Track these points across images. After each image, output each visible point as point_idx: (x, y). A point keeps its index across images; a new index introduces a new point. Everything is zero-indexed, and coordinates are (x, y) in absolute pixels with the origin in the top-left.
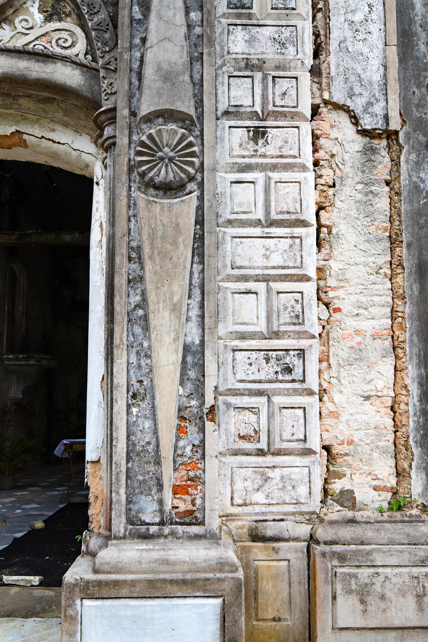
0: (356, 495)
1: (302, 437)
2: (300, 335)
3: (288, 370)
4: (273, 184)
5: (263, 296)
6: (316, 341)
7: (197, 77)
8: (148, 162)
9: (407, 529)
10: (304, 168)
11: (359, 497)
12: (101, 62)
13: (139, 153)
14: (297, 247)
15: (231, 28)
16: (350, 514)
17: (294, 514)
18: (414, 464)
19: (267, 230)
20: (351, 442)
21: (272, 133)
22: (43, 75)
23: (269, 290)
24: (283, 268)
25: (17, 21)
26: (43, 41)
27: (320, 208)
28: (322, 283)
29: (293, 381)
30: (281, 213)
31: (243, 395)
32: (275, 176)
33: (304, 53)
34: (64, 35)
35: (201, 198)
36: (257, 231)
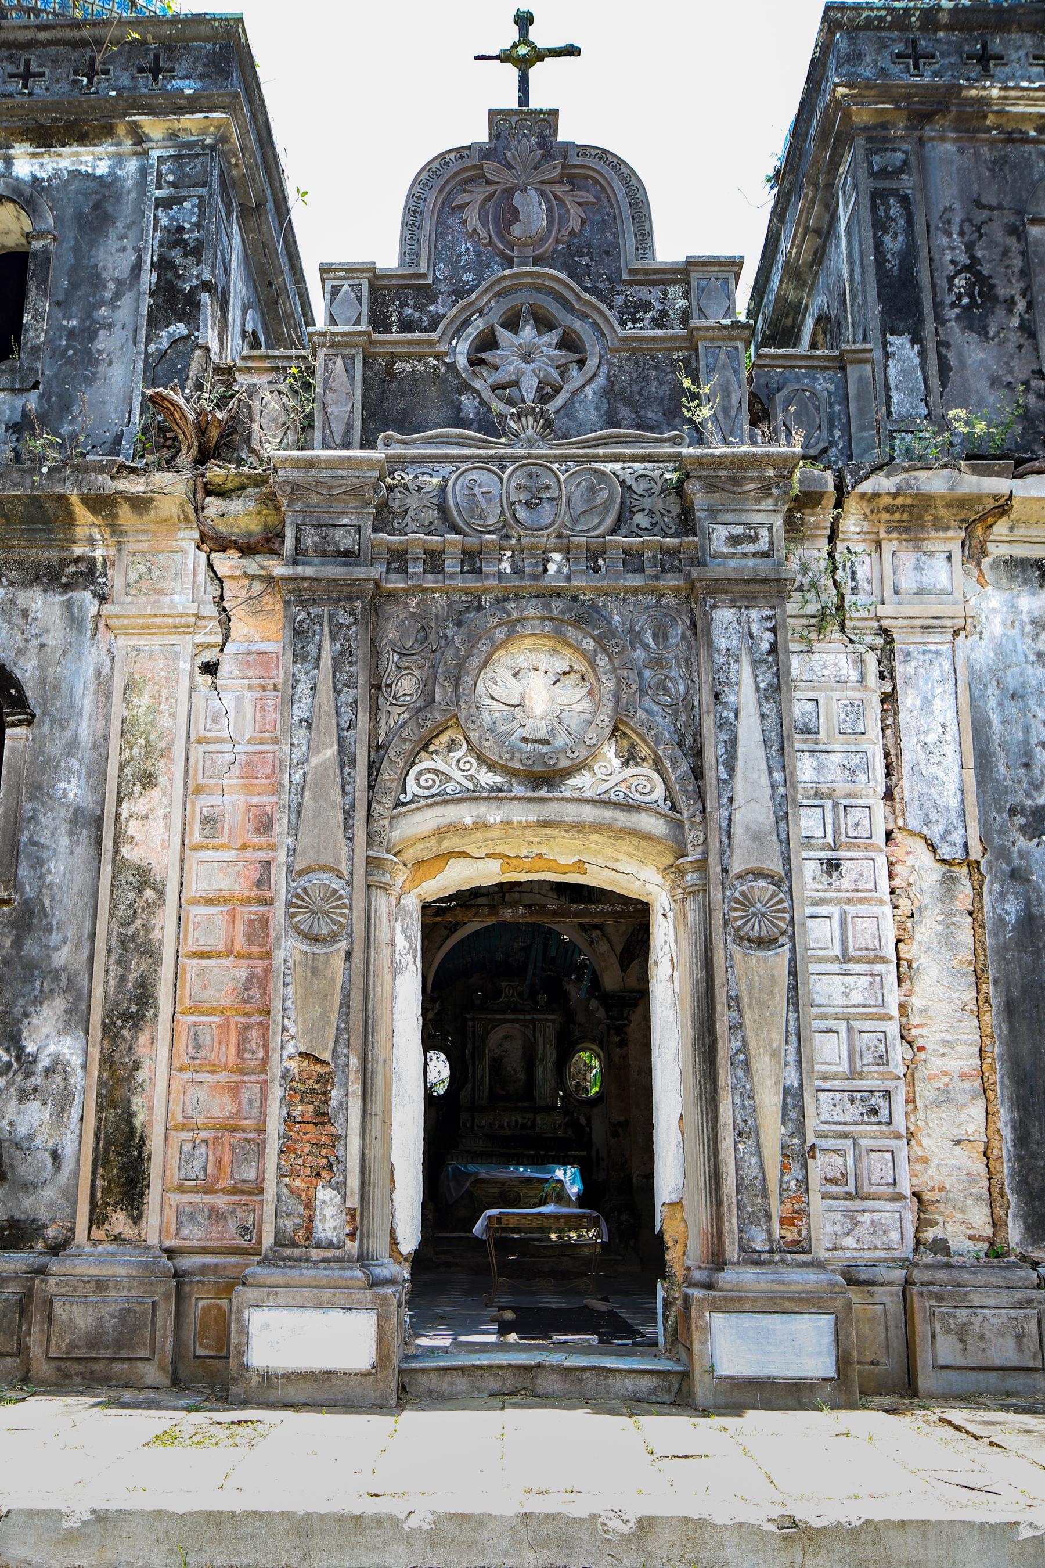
0: (950, 1244)
1: (891, 1180)
2: (883, 1077)
3: (874, 1112)
4: (849, 919)
5: (844, 1035)
6: (902, 1081)
7: (783, 835)
8: (742, 917)
13: (735, 910)
14: (877, 985)
16: (945, 1259)
17: (885, 1260)
19: (845, 966)
21: (846, 865)
22: (629, 824)
23: (849, 1029)
25: (596, 767)
26: (623, 787)
27: (899, 941)
28: (904, 1020)
29: (880, 1123)
30: (859, 949)
31: (827, 1136)
32: (851, 910)
33: (876, 781)
34: (643, 781)
35: (793, 950)
36: (835, 967)
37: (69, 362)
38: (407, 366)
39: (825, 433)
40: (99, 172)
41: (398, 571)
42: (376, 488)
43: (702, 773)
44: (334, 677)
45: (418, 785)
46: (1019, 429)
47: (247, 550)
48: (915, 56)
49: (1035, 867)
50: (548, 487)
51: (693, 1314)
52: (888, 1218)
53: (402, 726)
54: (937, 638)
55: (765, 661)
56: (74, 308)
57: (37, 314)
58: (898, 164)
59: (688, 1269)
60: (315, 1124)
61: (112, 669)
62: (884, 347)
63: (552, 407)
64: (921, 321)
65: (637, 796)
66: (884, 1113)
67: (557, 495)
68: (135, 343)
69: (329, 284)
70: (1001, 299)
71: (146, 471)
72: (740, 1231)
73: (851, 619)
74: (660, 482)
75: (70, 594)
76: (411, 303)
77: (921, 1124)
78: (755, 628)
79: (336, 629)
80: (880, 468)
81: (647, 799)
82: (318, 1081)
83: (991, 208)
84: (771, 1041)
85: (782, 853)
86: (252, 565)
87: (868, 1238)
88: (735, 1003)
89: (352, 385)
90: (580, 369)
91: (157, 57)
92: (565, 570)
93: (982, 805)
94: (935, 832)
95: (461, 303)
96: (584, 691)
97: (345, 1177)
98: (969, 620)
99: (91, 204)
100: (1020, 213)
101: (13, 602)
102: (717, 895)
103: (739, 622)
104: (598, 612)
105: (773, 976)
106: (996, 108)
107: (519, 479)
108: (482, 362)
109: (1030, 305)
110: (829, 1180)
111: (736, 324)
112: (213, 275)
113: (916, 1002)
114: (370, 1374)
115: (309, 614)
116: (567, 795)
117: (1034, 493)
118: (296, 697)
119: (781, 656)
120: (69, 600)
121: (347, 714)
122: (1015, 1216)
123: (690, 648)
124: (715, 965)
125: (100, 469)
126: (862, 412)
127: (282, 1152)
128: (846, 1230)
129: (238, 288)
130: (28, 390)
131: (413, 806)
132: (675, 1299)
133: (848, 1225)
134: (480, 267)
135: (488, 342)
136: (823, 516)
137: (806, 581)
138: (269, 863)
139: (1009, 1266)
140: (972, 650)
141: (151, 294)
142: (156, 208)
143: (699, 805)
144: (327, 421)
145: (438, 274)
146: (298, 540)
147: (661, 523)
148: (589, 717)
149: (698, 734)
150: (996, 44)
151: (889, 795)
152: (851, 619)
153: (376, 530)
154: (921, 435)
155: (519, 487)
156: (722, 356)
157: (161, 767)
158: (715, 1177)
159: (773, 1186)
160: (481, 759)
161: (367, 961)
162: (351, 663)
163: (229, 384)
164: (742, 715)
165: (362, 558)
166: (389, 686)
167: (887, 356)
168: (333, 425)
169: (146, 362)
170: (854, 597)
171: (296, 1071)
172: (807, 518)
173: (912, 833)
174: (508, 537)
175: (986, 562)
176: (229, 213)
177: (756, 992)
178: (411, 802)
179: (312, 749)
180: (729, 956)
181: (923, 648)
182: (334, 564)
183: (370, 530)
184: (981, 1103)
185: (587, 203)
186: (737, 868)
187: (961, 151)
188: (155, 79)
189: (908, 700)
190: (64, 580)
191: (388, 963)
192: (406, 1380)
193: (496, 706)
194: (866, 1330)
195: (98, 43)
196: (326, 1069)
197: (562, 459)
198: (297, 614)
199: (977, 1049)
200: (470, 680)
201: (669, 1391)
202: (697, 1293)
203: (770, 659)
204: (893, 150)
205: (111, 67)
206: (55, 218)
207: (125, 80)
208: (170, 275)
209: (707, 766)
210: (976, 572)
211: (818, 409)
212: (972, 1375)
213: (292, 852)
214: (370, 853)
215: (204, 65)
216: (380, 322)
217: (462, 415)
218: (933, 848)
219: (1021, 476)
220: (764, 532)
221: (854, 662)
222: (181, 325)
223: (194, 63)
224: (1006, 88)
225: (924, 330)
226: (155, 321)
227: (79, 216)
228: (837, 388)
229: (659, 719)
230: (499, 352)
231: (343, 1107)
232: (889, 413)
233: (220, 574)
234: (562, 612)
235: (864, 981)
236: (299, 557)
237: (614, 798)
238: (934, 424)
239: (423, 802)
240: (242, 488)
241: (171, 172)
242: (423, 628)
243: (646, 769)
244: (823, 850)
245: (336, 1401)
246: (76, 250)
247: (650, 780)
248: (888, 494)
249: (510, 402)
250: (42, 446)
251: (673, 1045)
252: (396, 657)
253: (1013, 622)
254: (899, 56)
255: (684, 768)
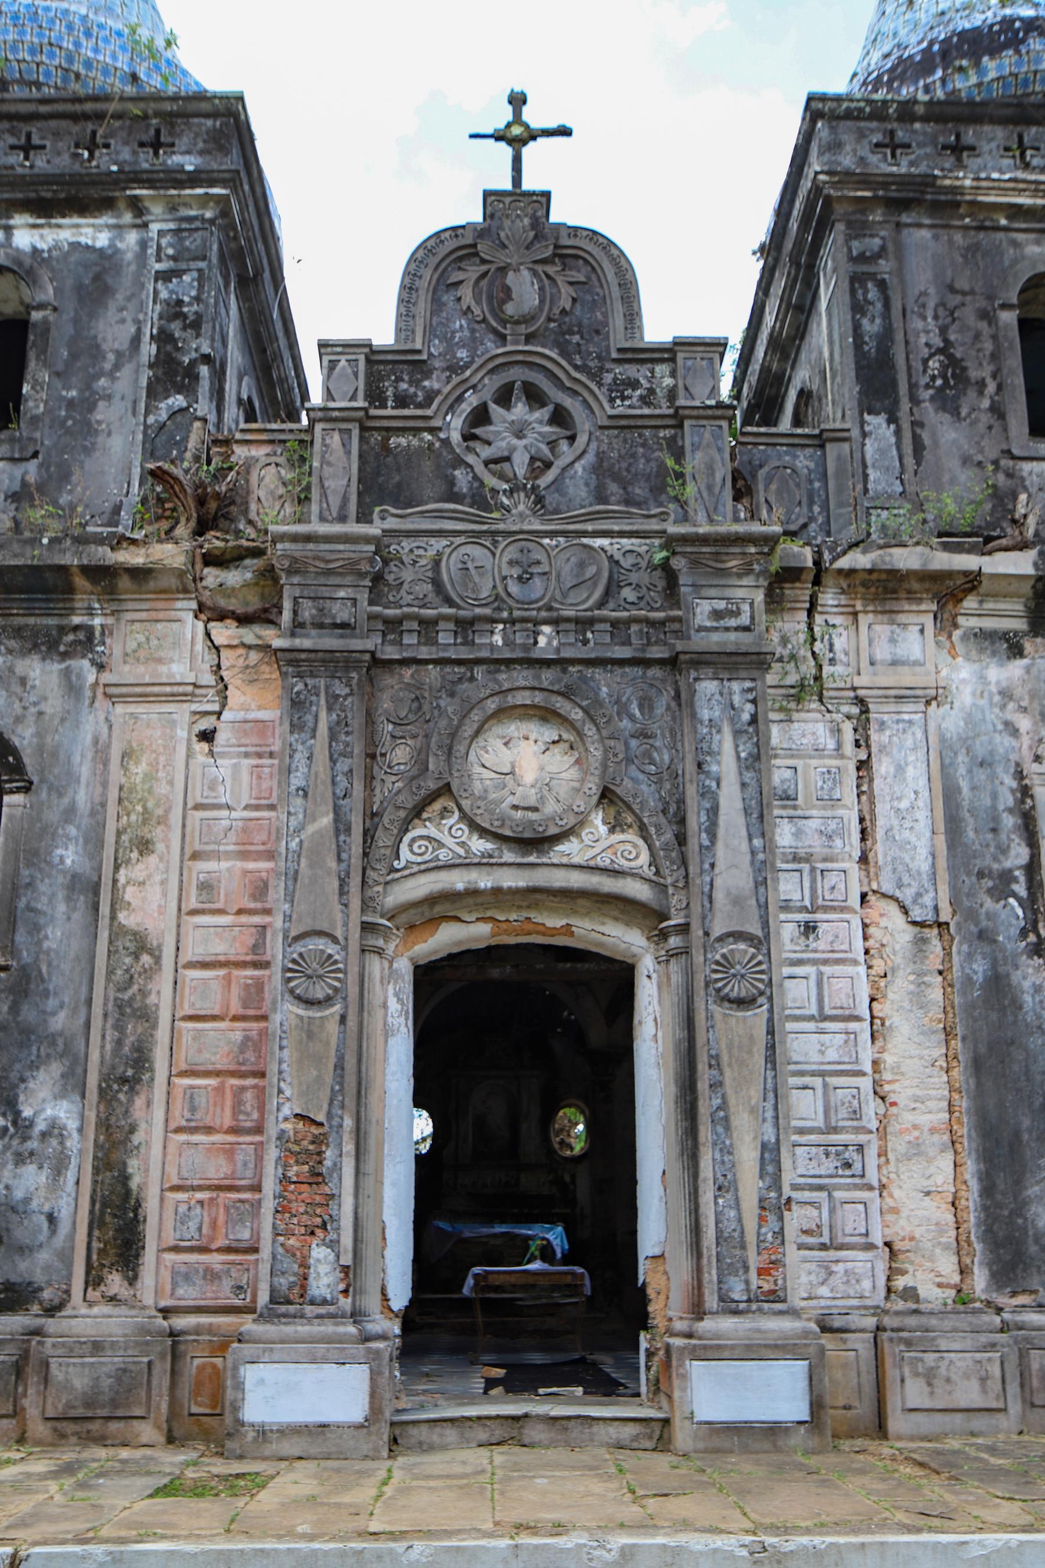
2: (858, 1130)
3: (848, 1165)
4: (825, 979)
5: (820, 1091)
9: (970, 1318)
10: (855, 962)
11: (922, 1293)
12: (669, 880)
14: (851, 1043)
15: (778, 820)
18: (976, 1260)
20: (912, 1239)
21: (822, 927)
23: (825, 1085)
24: (839, 1063)
26: (609, 854)
27: (872, 1000)
28: (877, 1076)
29: (853, 1176)
30: (835, 1008)
32: (827, 970)
33: (851, 845)
34: (629, 847)
36: (811, 1026)
37: (68, 432)
38: (403, 441)
39: (805, 509)
40: (99, 244)
41: (393, 643)
42: (372, 561)
43: (685, 839)
44: (330, 746)
45: (412, 851)
46: (988, 506)
47: (244, 620)
48: (892, 146)
49: (1002, 928)
50: (538, 563)
51: (674, 1363)
52: (861, 1268)
53: (397, 794)
54: (910, 707)
55: (746, 732)
56: (74, 379)
57: (36, 384)
58: (876, 249)
59: (670, 1320)
60: (310, 1184)
61: (110, 736)
62: (862, 427)
63: (544, 481)
64: (896, 402)
65: (623, 862)
66: (857, 1167)
67: (547, 569)
68: (134, 414)
69: (326, 359)
70: (973, 381)
71: (145, 542)
72: (720, 1282)
73: (828, 689)
74: (647, 558)
75: (68, 662)
76: (406, 378)
77: (893, 1176)
78: (737, 699)
79: (333, 700)
80: (856, 545)
81: (633, 864)
82: (313, 1142)
83: (964, 293)
84: (750, 1098)
85: (761, 917)
86: (249, 635)
87: (842, 1288)
88: (715, 1063)
89: (349, 459)
90: (571, 445)
91: (158, 132)
92: (555, 643)
93: (952, 869)
94: (907, 895)
95: (456, 379)
96: (573, 760)
97: (339, 1235)
98: (940, 691)
99: (91, 275)
100: (991, 298)
101: (11, 670)
102: (698, 958)
103: (721, 694)
104: (586, 683)
105: (752, 1036)
106: (968, 198)
107: (512, 553)
108: (474, 437)
109: (1000, 388)
110: (805, 1232)
111: (720, 405)
112: (213, 349)
113: (889, 1059)
114: (361, 1426)
115: (306, 685)
116: (555, 861)
117: (1001, 570)
118: (293, 766)
119: (761, 727)
120: (67, 668)
121: (342, 782)
122: (981, 1264)
123: (674, 719)
124: (697, 1025)
125: (99, 540)
126: (841, 488)
127: (277, 1211)
128: (821, 1280)
129: (235, 356)
130: (27, 460)
131: (406, 872)
132: (658, 1349)
133: (823, 1275)
134: (473, 344)
135: (480, 416)
136: (802, 592)
137: (786, 652)
138: (264, 927)
139: (975, 1312)
140: (944, 719)
141: (151, 366)
142: (156, 281)
143: (682, 871)
144: (324, 495)
145: (432, 350)
146: (295, 613)
147: (647, 598)
148: (576, 785)
149: (681, 802)
150: (969, 135)
151: (864, 859)
152: (828, 689)
153: (371, 603)
154: (896, 512)
155: (511, 563)
156: (707, 435)
157: (158, 833)
158: (696, 1230)
159: (751, 1238)
160: (475, 827)
161: (361, 1024)
162: (347, 733)
163: (227, 457)
164: (723, 784)
165: (358, 631)
166: (383, 755)
167: (864, 435)
168: (330, 499)
169: (145, 433)
170: (832, 668)
171: (291, 1133)
172: (787, 592)
173: (884, 896)
174: (499, 609)
175: (957, 634)
176: (227, 285)
177: (735, 1051)
178: (405, 868)
179: (310, 817)
180: (710, 1017)
181: (896, 717)
182: (331, 636)
183: (366, 603)
184: (950, 1156)
185: (578, 283)
186: (717, 931)
187: (936, 237)
188: (156, 154)
189: (882, 767)
190: (62, 648)
191: (380, 1025)
192: (397, 1432)
193: (487, 774)
194: (839, 1375)
195: (100, 116)
196: (321, 1130)
197: (552, 534)
198: (293, 685)
199: (946, 1103)
200: (462, 749)
201: (651, 1438)
202: (677, 1342)
203: (751, 730)
204: (872, 236)
205: (112, 142)
206: (55, 289)
207: (126, 154)
208: (169, 348)
209: (689, 833)
210: (948, 644)
211: (798, 485)
212: (938, 1417)
213: (288, 918)
214: (365, 919)
215: (205, 141)
216: (375, 396)
217: (456, 489)
218: (906, 912)
219: (990, 553)
220: (746, 607)
221: (832, 731)
222: (180, 397)
223: (195, 139)
224: (978, 179)
225: (899, 410)
226: (155, 392)
227: (79, 287)
228: (817, 465)
229: (644, 787)
230: (492, 428)
231: (337, 1167)
232: (866, 490)
233: (216, 643)
234: (552, 683)
235: (840, 1039)
236: (298, 626)
237: (601, 864)
238: (909, 501)
239: (416, 869)
240: (241, 558)
241: (171, 245)
242: (417, 698)
243: (631, 836)
244: (800, 912)
245: (330, 1454)
246: (76, 321)
247: (635, 846)
248: (864, 570)
249: (502, 477)
250: (42, 517)
251: (657, 1102)
252: (391, 727)
253: (982, 693)
254: (878, 145)
255: (669, 836)
